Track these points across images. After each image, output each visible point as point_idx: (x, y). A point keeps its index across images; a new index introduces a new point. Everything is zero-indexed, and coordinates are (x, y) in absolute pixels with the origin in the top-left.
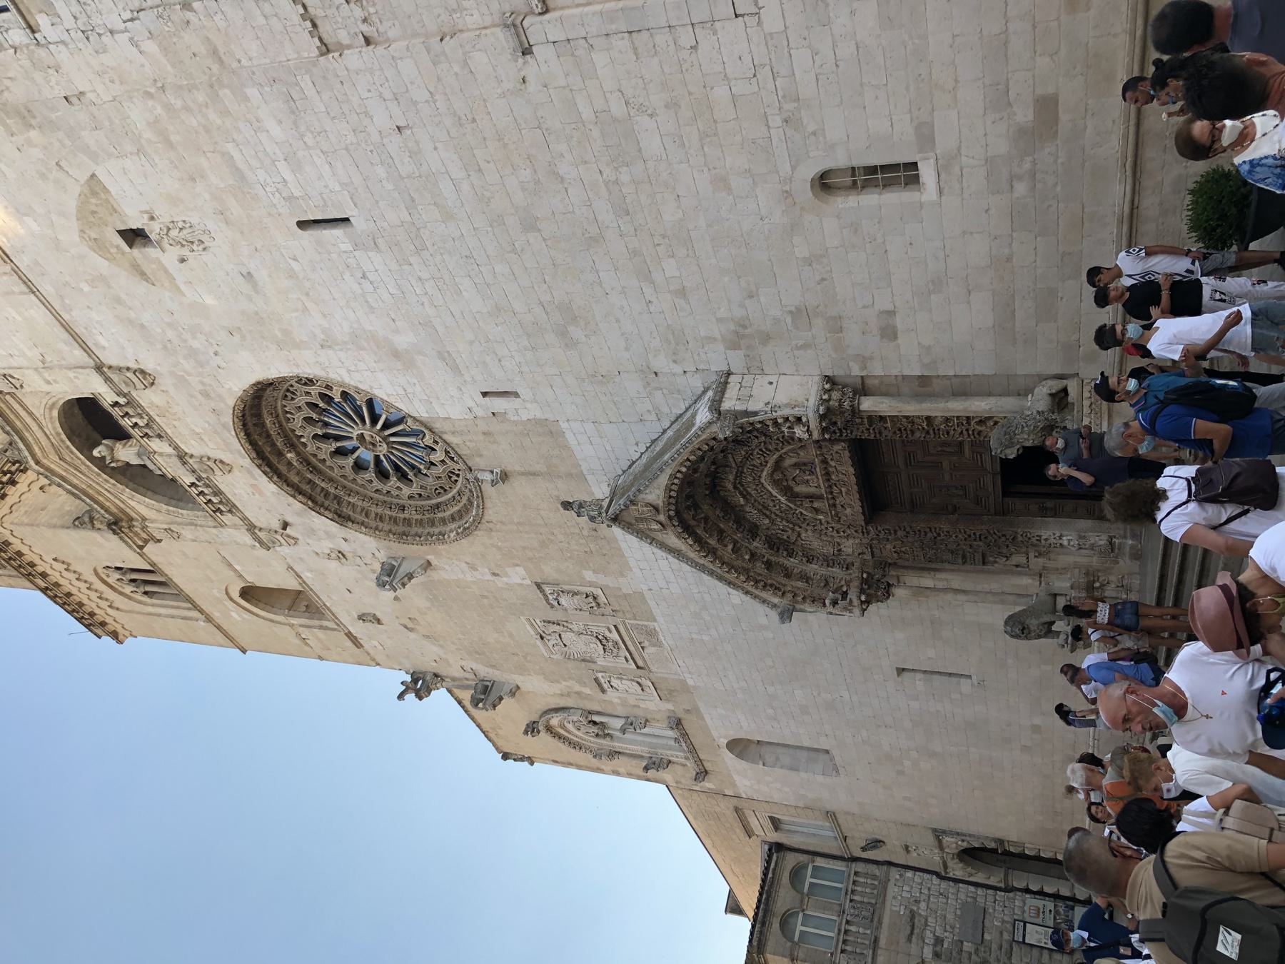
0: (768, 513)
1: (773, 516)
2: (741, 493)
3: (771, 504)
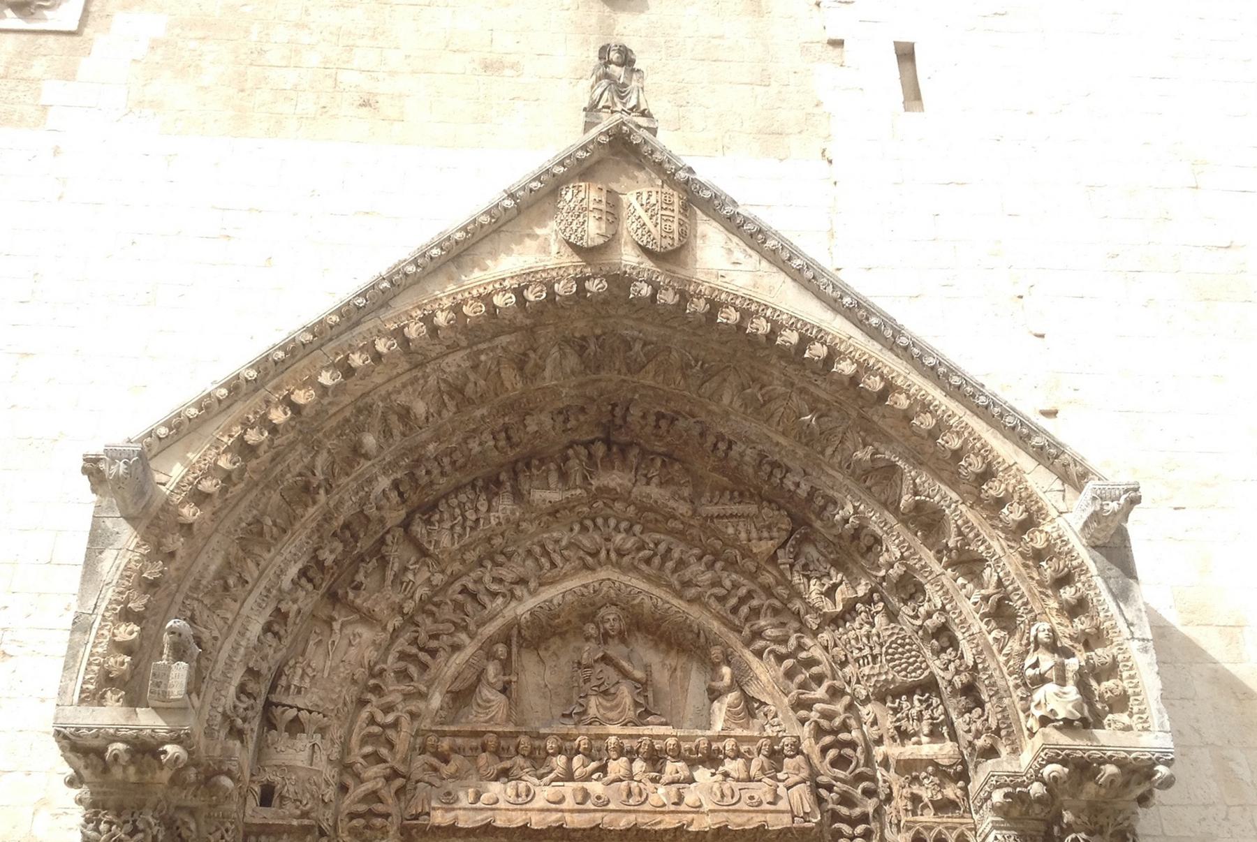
1: (457, 566)
2: (568, 505)
3: (508, 574)
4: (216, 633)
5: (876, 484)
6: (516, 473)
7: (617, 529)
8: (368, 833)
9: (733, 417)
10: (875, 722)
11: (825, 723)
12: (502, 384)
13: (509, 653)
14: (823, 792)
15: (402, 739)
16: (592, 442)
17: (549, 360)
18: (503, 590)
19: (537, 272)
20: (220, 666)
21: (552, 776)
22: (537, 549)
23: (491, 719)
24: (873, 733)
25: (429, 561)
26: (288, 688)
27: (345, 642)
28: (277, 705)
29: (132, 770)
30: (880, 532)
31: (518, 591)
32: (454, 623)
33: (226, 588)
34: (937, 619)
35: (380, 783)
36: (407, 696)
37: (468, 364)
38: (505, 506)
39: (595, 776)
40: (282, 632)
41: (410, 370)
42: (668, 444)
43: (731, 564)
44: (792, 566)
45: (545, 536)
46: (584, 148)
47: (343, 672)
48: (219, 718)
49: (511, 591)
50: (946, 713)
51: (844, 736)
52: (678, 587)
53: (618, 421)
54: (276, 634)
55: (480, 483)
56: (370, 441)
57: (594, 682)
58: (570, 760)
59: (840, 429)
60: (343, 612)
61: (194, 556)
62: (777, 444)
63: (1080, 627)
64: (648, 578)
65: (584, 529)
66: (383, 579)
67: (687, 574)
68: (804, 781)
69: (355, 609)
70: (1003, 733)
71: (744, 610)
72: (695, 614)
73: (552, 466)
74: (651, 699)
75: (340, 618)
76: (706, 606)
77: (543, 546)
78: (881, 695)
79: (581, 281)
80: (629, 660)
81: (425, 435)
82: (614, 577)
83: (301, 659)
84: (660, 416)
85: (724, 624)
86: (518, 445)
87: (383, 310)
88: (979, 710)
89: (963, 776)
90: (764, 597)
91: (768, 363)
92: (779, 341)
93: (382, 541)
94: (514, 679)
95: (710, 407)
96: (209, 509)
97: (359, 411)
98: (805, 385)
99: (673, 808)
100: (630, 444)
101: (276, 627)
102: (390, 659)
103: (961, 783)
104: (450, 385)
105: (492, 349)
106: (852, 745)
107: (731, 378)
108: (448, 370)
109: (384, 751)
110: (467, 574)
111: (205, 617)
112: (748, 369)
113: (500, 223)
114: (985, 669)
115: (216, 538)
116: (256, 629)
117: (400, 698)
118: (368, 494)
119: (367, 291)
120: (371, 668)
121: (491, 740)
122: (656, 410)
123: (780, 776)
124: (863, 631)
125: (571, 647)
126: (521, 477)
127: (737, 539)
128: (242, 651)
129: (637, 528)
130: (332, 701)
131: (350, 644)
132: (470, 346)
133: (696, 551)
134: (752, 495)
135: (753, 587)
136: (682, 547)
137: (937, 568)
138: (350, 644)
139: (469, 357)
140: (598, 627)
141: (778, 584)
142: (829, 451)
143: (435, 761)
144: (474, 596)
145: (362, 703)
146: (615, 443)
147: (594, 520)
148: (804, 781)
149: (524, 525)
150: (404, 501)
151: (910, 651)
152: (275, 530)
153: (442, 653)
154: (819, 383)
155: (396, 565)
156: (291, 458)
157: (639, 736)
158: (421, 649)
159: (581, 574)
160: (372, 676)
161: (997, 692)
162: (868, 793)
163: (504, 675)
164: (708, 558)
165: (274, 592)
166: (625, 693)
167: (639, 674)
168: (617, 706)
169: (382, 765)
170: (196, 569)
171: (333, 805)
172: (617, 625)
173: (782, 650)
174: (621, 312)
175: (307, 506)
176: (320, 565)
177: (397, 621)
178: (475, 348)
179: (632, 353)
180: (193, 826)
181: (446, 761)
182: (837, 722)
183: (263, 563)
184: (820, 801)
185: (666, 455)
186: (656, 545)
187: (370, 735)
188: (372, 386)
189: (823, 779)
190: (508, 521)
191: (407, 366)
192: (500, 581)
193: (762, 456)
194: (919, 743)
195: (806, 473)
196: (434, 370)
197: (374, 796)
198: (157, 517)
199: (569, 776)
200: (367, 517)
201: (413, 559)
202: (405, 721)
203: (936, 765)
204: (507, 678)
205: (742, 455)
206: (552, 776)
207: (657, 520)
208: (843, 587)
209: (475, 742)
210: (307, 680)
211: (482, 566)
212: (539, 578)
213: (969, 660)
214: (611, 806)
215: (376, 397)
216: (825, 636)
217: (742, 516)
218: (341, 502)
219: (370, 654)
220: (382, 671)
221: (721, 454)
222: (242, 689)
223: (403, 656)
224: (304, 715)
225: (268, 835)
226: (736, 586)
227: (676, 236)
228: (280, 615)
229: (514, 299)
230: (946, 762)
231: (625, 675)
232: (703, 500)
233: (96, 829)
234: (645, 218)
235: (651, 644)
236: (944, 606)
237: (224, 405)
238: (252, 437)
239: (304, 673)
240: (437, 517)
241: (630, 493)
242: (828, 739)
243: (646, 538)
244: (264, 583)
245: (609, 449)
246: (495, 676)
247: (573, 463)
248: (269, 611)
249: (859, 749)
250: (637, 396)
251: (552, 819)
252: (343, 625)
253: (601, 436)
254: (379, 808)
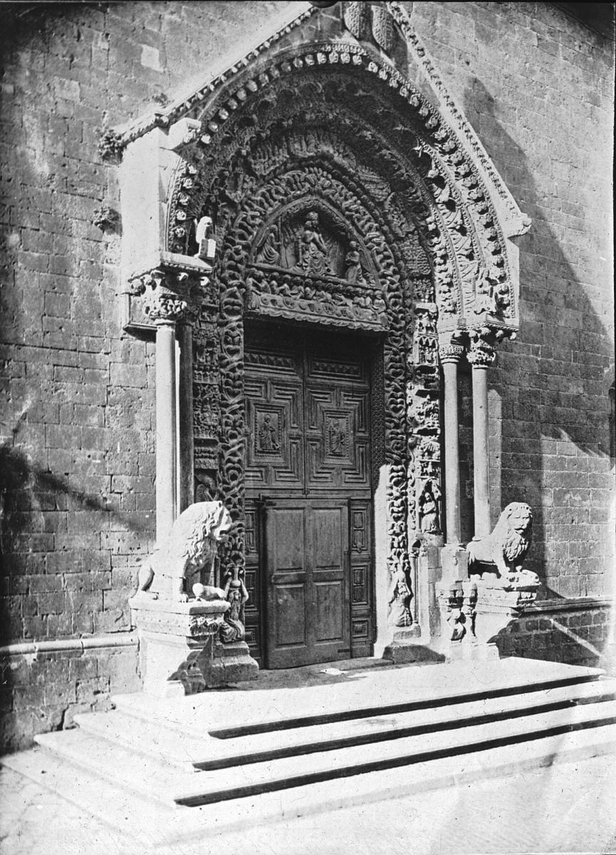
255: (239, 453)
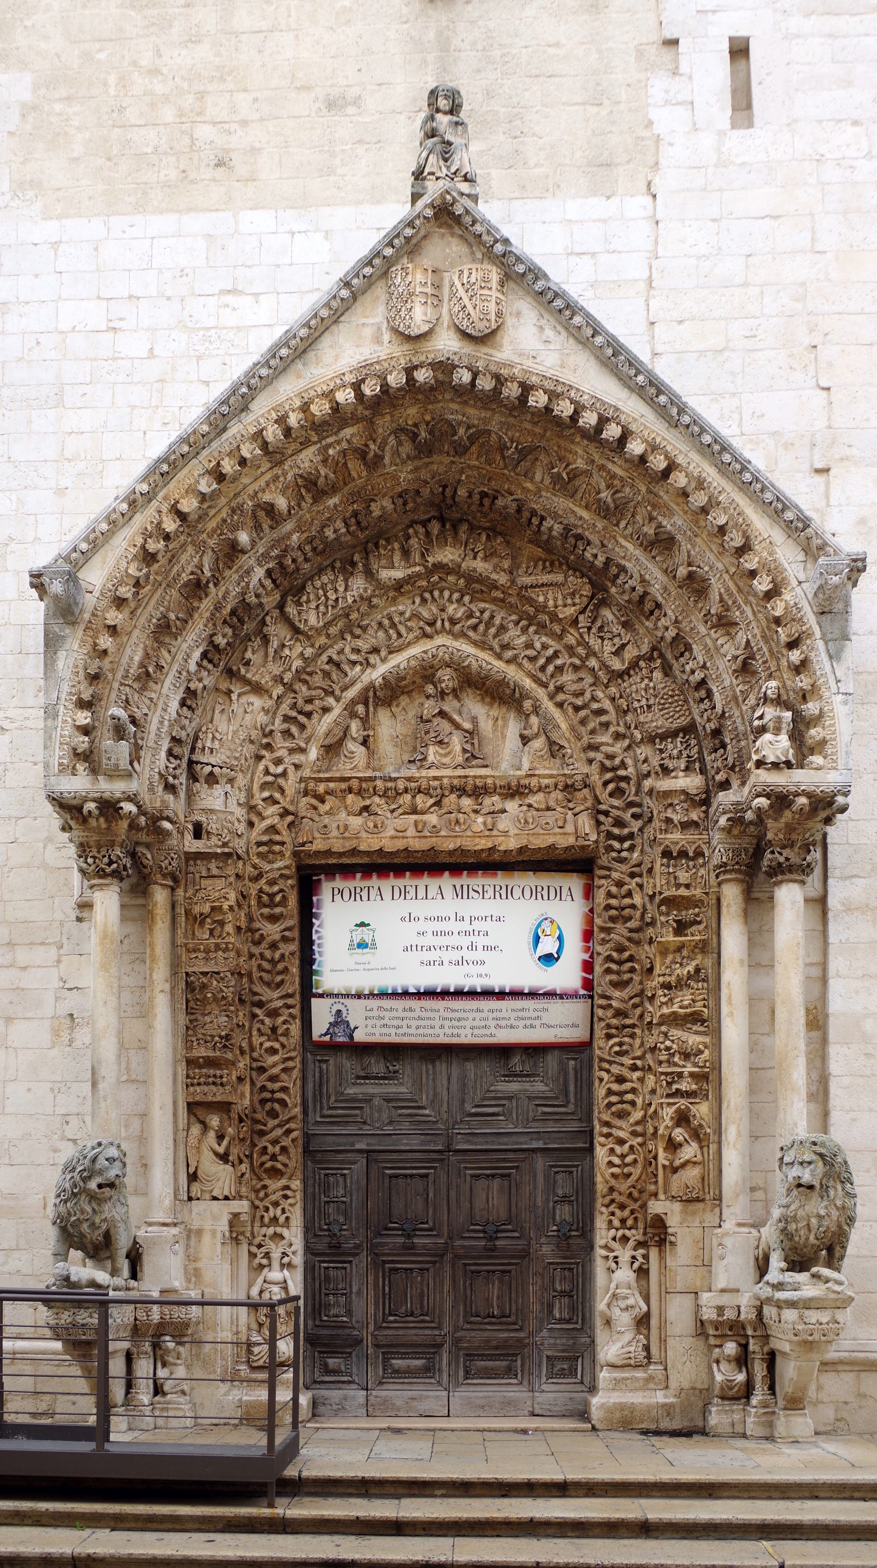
0: (333, 630)
2: (409, 580)
4: (145, 711)
5: (660, 553)
6: (367, 554)
7: (450, 600)
8: (271, 856)
9: (544, 493)
10: (645, 761)
11: (608, 763)
12: (350, 474)
13: (367, 712)
14: (602, 818)
15: (291, 784)
16: (429, 520)
17: (387, 448)
18: (361, 659)
19: (372, 364)
20: (152, 736)
21: (400, 811)
22: (386, 622)
23: (355, 767)
24: (645, 768)
25: (301, 637)
26: (203, 749)
27: (241, 710)
28: (197, 763)
29: (102, 820)
30: (660, 599)
31: (373, 659)
32: (324, 690)
33: (148, 674)
34: (698, 676)
35: (276, 819)
36: (291, 751)
37: (319, 458)
38: (359, 584)
39: (432, 810)
40: (194, 706)
41: (271, 468)
42: (491, 521)
43: (542, 626)
44: (589, 629)
45: (393, 609)
46: (411, 224)
47: (242, 735)
48: (157, 777)
49: (367, 659)
50: (700, 752)
51: (621, 773)
52: (498, 650)
53: (449, 501)
54: (189, 708)
55: (338, 564)
56: (243, 537)
57: (433, 734)
58: (414, 797)
59: (632, 504)
60: (238, 685)
61: (120, 648)
62: (581, 518)
63: (800, 684)
64: (475, 643)
65: (424, 601)
66: (266, 655)
67: (506, 638)
68: (587, 809)
69: (248, 682)
70: (737, 769)
71: (550, 668)
72: (512, 673)
73: (396, 545)
74: (476, 746)
75: (237, 688)
76: (520, 665)
77: (390, 619)
78: (651, 739)
79: (409, 371)
80: (460, 714)
81: (289, 526)
82: (448, 644)
83: (210, 726)
84: (483, 495)
85: (535, 681)
86: (367, 528)
87: (244, 414)
88: (722, 750)
89: (706, 802)
90: (567, 657)
91: (573, 442)
92: (581, 422)
93: (263, 623)
94: (371, 733)
95: (525, 485)
96: (126, 612)
97: (233, 511)
98: (604, 462)
99: (487, 833)
100: (461, 521)
101: (189, 702)
102: (278, 721)
103: (704, 808)
104: (305, 479)
105: (339, 442)
106: (626, 779)
107: (542, 457)
108: (302, 466)
109: (277, 795)
110: (331, 646)
111: (136, 699)
112: (555, 448)
113: (339, 313)
114: (730, 717)
115: (136, 633)
116: (174, 705)
117: (287, 753)
118: (248, 584)
119: (229, 398)
120: (263, 729)
121: (355, 784)
122: (482, 489)
123: (571, 805)
124: (643, 685)
125: (417, 702)
126: (371, 556)
127: (546, 607)
128: (166, 723)
129: (467, 599)
130: (236, 758)
131: (246, 712)
132: (320, 441)
133: (514, 617)
134: (561, 564)
135: (558, 647)
136: (503, 614)
137: (703, 630)
138: (246, 712)
139: (319, 450)
140: (436, 687)
141: (579, 644)
142: (623, 524)
143: (314, 802)
144: (338, 665)
145: (259, 758)
146: (449, 520)
147: (431, 593)
148: (587, 809)
149: (375, 601)
150: (277, 586)
151: (677, 701)
152: (178, 623)
153: (315, 715)
154: (616, 459)
155: (276, 643)
156: (184, 558)
157: (466, 777)
158: (300, 713)
159: (422, 642)
160: (265, 736)
161: (737, 735)
162: (635, 816)
163: (365, 730)
164: (524, 623)
165: (184, 673)
166: (456, 742)
167: (467, 726)
168: (449, 753)
169: (277, 806)
170: (125, 660)
171: (245, 837)
172: (451, 685)
173: (579, 702)
174: (448, 396)
175: (201, 599)
176: (216, 647)
177: (278, 690)
178: (324, 443)
179: (456, 438)
180: (149, 856)
181: (323, 801)
182: (617, 761)
183: (172, 650)
184: (599, 823)
185: (489, 529)
186: (482, 612)
187: (266, 783)
188: (241, 487)
189: (603, 807)
190: (362, 598)
191: (269, 465)
192: (357, 651)
193: (567, 529)
194: (676, 777)
195: (603, 546)
196: (291, 467)
197: (272, 829)
198: (90, 622)
199: (414, 811)
200: (248, 604)
201: (288, 637)
202: (291, 770)
203: (688, 794)
204: (366, 733)
205: (551, 529)
206: (400, 811)
207: (482, 591)
208: (629, 647)
209: (344, 786)
210: (217, 742)
211: (344, 639)
212: (388, 647)
213: (719, 709)
214: (443, 833)
215: (246, 497)
216: (613, 690)
217: (551, 584)
218: (227, 592)
219: (262, 718)
220: (272, 731)
221: (534, 528)
222: (170, 753)
223: (287, 719)
224: (217, 770)
225: (202, 859)
226: (545, 647)
227: (493, 317)
228: (190, 693)
229: (352, 395)
230: (695, 792)
231: (457, 726)
232: (520, 572)
233: (86, 862)
234: (466, 300)
235: (479, 698)
236: (705, 663)
237: (127, 518)
238: (152, 546)
239: (214, 738)
240: (305, 598)
241: (460, 567)
242: (609, 775)
243: (472, 606)
244: (176, 667)
245: (444, 526)
246: (358, 731)
247: (414, 542)
248: (182, 689)
249: (632, 782)
250: (463, 477)
251: (400, 845)
252: (239, 695)
253: (436, 514)
254: (277, 838)
255: (284, 1076)
